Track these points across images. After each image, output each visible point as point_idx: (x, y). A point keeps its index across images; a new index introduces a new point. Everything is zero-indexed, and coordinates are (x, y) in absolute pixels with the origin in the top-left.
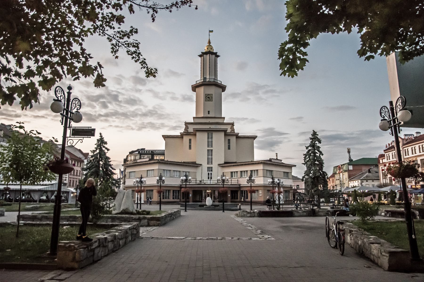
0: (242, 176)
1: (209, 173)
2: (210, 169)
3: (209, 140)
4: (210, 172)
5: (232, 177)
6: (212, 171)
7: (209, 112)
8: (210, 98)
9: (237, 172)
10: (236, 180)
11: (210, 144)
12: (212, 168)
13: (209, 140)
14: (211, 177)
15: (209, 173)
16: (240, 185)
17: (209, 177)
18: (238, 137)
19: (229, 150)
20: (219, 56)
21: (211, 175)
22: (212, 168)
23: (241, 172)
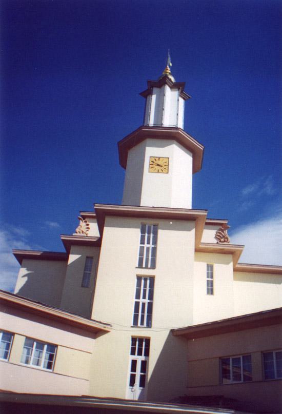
1: (134, 363)
3: (146, 245)
4: (140, 359)
6: (147, 354)
11: (148, 259)
17: (133, 378)
19: (210, 296)
22: (148, 341)
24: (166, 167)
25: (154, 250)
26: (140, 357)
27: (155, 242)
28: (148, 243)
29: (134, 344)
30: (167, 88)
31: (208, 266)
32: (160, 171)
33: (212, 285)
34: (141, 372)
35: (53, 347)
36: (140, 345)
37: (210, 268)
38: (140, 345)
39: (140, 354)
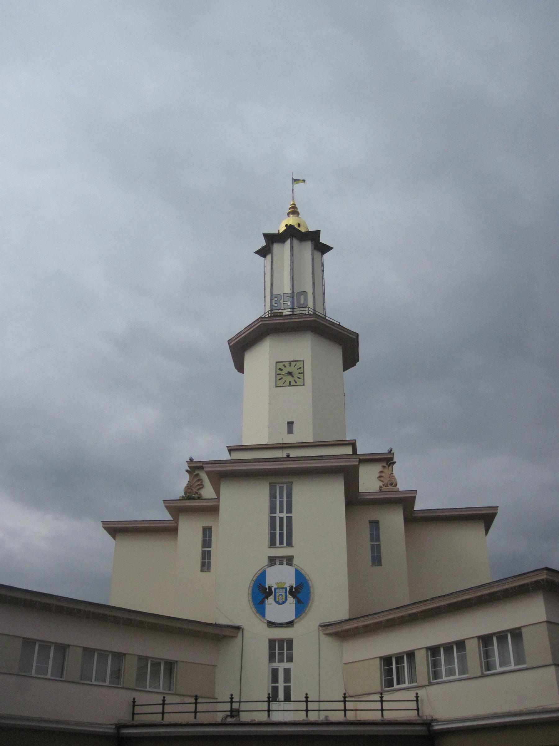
0: (436, 675)
1: (275, 672)
2: (280, 649)
3: (278, 515)
4: (281, 667)
5: (390, 683)
6: (290, 660)
7: (290, 424)
8: (296, 374)
9: (411, 655)
10: (411, 695)
11: (280, 532)
13: (278, 515)
14: (287, 691)
15: (275, 672)
16: (428, 724)
18: (416, 520)
19: (377, 569)
20: (324, 249)
21: (287, 679)
22: (290, 642)
23: (434, 651)
24: (301, 376)
25: (289, 519)
27: (289, 510)
28: (281, 511)
30: (295, 241)
31: (370, 522)
32: (293, 383)
33: (379, 552)
34: (285, 683)
35: (170, 666)
36: (281, 648)
37: (375, 524)
38: (281, 648)
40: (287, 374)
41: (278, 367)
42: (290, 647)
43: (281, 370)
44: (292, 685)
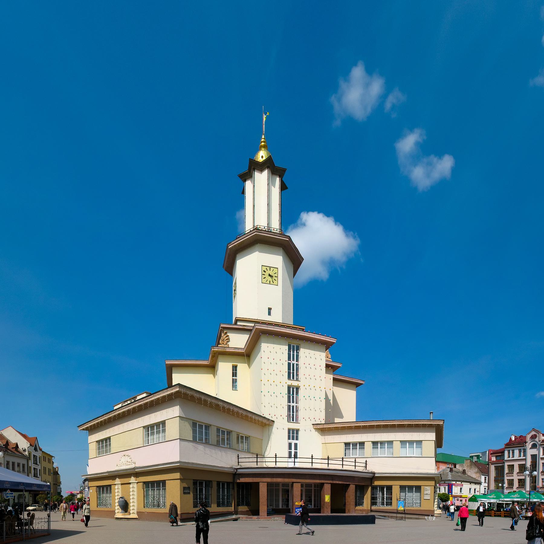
1: (290, 445)
2: (293, 434)
4: (293, 442)
6: (297, 439)
12: (298, 431)
14: (296, 454)
17: (290, 453)
21: (296, 448)
22: (298, 431)
24: (276, 278)
26: (293, 441)
29: (289, 433)
36: (293, 433)
38: (293, 433)
39: (293, 439)
40: (268, 275)
41: (263, 270)
42: (297, 433)
43: (264, 271)
44: (298, 451)
